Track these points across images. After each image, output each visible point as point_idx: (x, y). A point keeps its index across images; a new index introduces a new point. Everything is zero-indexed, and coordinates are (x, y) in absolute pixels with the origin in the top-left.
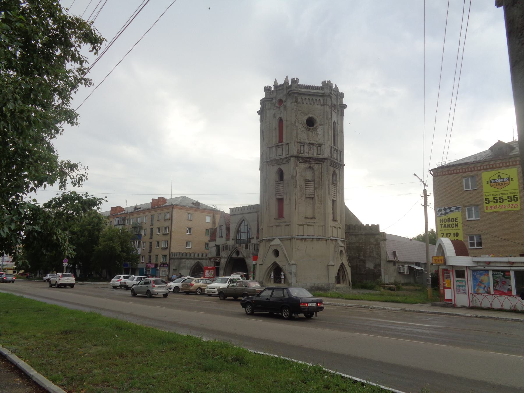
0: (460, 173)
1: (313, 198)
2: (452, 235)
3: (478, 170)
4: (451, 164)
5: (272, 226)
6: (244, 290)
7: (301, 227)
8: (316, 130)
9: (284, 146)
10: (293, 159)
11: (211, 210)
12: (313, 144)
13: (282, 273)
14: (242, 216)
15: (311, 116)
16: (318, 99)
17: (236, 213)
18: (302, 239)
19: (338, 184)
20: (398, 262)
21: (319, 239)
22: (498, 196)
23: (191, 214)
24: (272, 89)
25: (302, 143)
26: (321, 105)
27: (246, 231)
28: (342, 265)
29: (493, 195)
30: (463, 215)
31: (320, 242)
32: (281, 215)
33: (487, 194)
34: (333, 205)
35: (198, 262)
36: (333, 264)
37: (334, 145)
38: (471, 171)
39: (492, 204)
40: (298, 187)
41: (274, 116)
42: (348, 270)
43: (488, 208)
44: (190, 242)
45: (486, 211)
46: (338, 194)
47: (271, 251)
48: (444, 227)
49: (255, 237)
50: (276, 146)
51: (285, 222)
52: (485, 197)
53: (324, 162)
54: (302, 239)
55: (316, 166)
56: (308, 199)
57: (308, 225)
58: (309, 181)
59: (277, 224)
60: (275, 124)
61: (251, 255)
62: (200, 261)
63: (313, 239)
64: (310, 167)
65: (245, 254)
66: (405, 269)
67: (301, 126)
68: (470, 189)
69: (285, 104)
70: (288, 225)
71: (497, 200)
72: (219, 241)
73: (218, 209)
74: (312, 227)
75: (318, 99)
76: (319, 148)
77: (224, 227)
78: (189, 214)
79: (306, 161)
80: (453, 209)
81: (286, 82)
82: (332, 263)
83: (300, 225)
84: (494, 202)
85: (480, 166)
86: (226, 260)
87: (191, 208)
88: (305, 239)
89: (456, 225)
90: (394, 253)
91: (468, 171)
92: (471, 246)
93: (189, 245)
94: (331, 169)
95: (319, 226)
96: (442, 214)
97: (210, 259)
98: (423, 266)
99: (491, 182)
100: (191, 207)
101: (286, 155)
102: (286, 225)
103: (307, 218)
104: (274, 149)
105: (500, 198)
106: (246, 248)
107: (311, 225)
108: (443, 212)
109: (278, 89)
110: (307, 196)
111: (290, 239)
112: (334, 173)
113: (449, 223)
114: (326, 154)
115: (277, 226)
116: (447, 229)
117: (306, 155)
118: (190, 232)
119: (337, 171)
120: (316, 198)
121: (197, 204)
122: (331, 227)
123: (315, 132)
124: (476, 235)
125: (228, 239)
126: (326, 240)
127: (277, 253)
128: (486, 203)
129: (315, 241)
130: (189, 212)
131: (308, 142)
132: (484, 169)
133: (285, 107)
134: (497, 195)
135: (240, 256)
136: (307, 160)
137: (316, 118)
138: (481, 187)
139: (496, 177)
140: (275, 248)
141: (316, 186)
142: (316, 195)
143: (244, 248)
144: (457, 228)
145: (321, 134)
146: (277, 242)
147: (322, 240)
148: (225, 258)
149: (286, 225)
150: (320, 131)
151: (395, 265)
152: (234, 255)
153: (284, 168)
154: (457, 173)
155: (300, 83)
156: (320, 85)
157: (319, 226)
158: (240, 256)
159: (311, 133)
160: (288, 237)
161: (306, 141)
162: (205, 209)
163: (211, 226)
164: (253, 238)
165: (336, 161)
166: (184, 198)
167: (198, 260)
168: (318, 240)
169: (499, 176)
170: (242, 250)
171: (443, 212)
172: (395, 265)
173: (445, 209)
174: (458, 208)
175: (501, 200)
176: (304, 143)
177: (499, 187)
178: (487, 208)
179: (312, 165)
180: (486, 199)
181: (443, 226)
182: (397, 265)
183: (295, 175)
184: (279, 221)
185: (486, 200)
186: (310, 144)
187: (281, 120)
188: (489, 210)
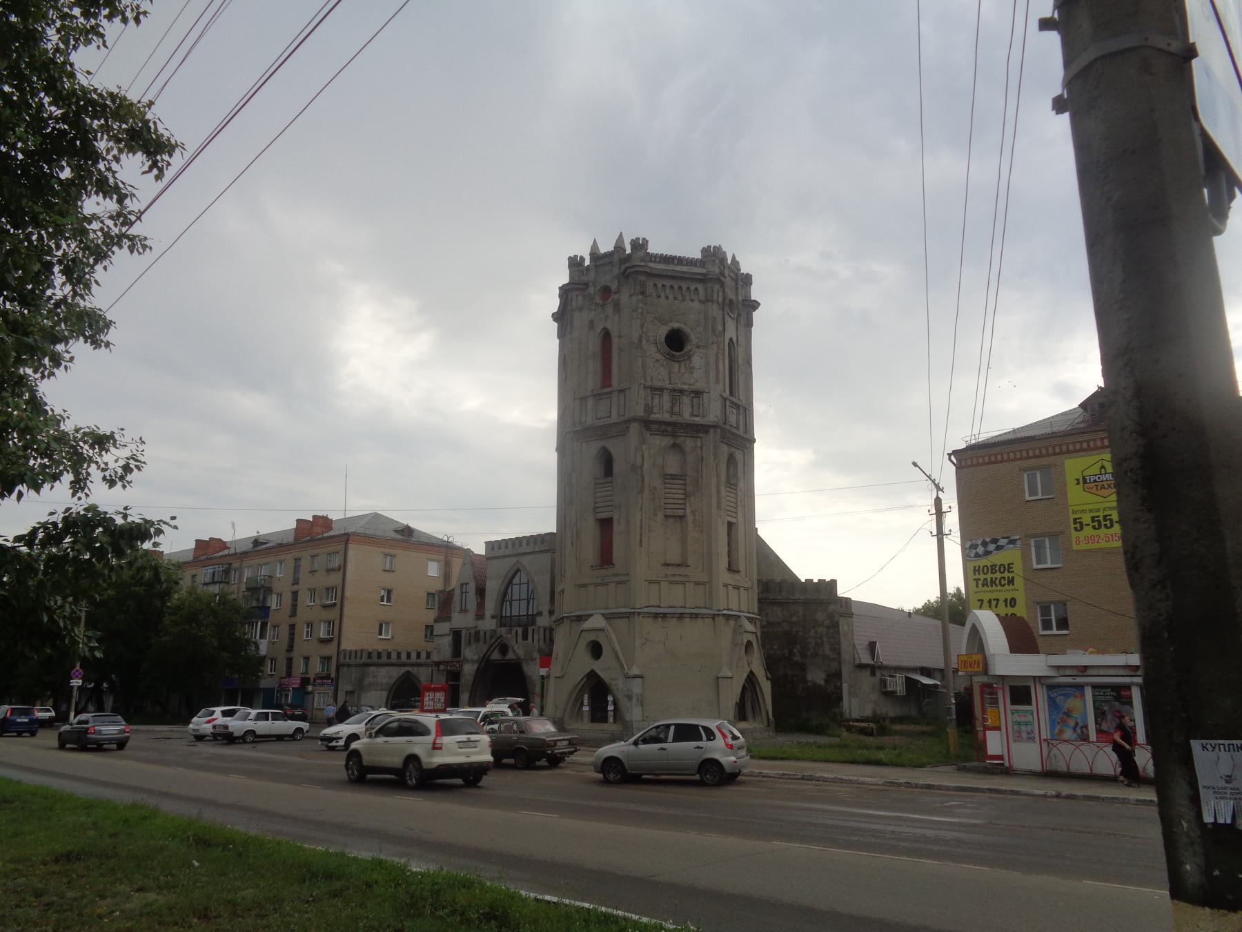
0: (1015, 459)
1: (682, 518)
2: (1001, 604)
3: (1055, 454)
4: (999, 439)
6: (517, 742)
7: (655, 586)
8: (689, 358)
9: (615, 396)
10: (634, 428)
11: (439, 546)
12: (682, 391)
13: (610, 698)
14: (514, 560)
15: (676, 325)
16: (692, 288)
17: (501, 553)
18: (656, 616)
19: (741, 485)
20: (882, 667)
22: (1101, 514)
23: (393, 556)
24: (587, 263)
25: (656, 389)
26: (700, 301)
27: (524, 596)
28: (751, 678)
29: (1091, 511)
30: (1026, 558)
31: (700, 621)
32: (606, 557)
33: (1076, 508)
34: (729, 535)
35: (408, 672)
36: (730, 674)
37: (731, 393)
38: (1041, 456)
39: (1088, 531)
40: (647, 491)
41: (591, 324)
42: (766, 687)
43: (1081, 541)
44: (387, 624)
45: (1075, 547)
46: (740, 509)
47: (583, 644)
49: (545, 609)
50: (594, 396)
51: (615, 575)
52: (1072, 516)
53: (707, 432)
54: (656, 616)
55: (689, 444)
56: (670, 520)
57: (671, 583)
58: (672, 477)
59: (599, 581)
60: (594, 344)
61: (536, 655)
62: (414, 670)
63: (681, 616)
64: (674, 446)
65: (521, 653)
66: (897, 685)
68: (1040, 496)
69: (616, 297)
71: (1099, 522)
72: (460, 620)
73: (459, 544)
74: (681, 586)
75: (692, 288)
76: (695, 400)
77: (472, 588)
78: (386, 555)
80: (1002, 542)
81: (619, 247)
83: (651, 582)
84: (1094, 527)
85: (1060, 446)
86: (475, 666)
87: (392, 543)
88: (664, 616)
89: (1011, 581)
90: (872, 646)
91: (1035, 457)
93: (387, 631)
94: (725, 449)
95: (697, 583)
96: (977, 555)
97: (438, 664)
98: (938, 675)
99: (1085, 481)
100: (393, 540)
101: (619, 416)
102: (620, 583)
103: (668, 565)
104: (590, 403)
105: (1105, 517)
106: (525, 637)
107: (676, 583)
108: (980, 550)
109: (601, 262)
110: (669, 512)
111: (628, 616)
112: (731, 459)
113: (994, 576)
114: (713, 414)
115: (597, 585)
116: (990, 588)
117: (667, 417)
118: (389, 600)
119: (739, 455)
120: (690, 518)
121: (407, 531)
122: (725, 585)
124: (1054, 603)
125: (480, 616)
126: (714, 617)
127: (596, 650)
128: (1076, 529)
129: (687, 620)
130: (387, 551)
131: (670, 387)
132: (1068, 452)
133: (617, 307)
134: (1098, 510)
135: (510, 656)
136: (669, 428)
137: (687, 330)
138: (1064, 493)
141: (689, 488)
142: (688, 510)
143: (520, 638)
144: (1011, 587)
145: (699, 368)
146: (597, 621)
147: (703, 616)
148: (473, 662)
149: (620, 583)
150: (697, 361)
151: (873, 674)
152: (496, 656)
153: (614, 447)
154: (1009, 460)
155: (653, 249)
156: (698, 256)
157: (697, 583)
158: (510, 656)
159: (676, 366)
160: (623, 610)
161: (666, 384)
162: (427, 544)
163: (439, 586)
164: (540, 614)
165: (735, 431)
166: (376, 517)
167: (407, 669)
168: (694, 616)
169: (1103, 467)
171: (980, 550)
172: (873, 674)
173: (985, 544)
174: (1013, 542)
175: (1108, 523)
176: (661, 390)
177: (1103, 492)
178: (1078, 539)
179: (679, 440)
180: (1075, 520)
182: (878, 674)
183: (639, 462)
184: (603, 572)
185: (1075, 523)
186: (674, 390)
187: (606, 336)
188: (1083, 546)
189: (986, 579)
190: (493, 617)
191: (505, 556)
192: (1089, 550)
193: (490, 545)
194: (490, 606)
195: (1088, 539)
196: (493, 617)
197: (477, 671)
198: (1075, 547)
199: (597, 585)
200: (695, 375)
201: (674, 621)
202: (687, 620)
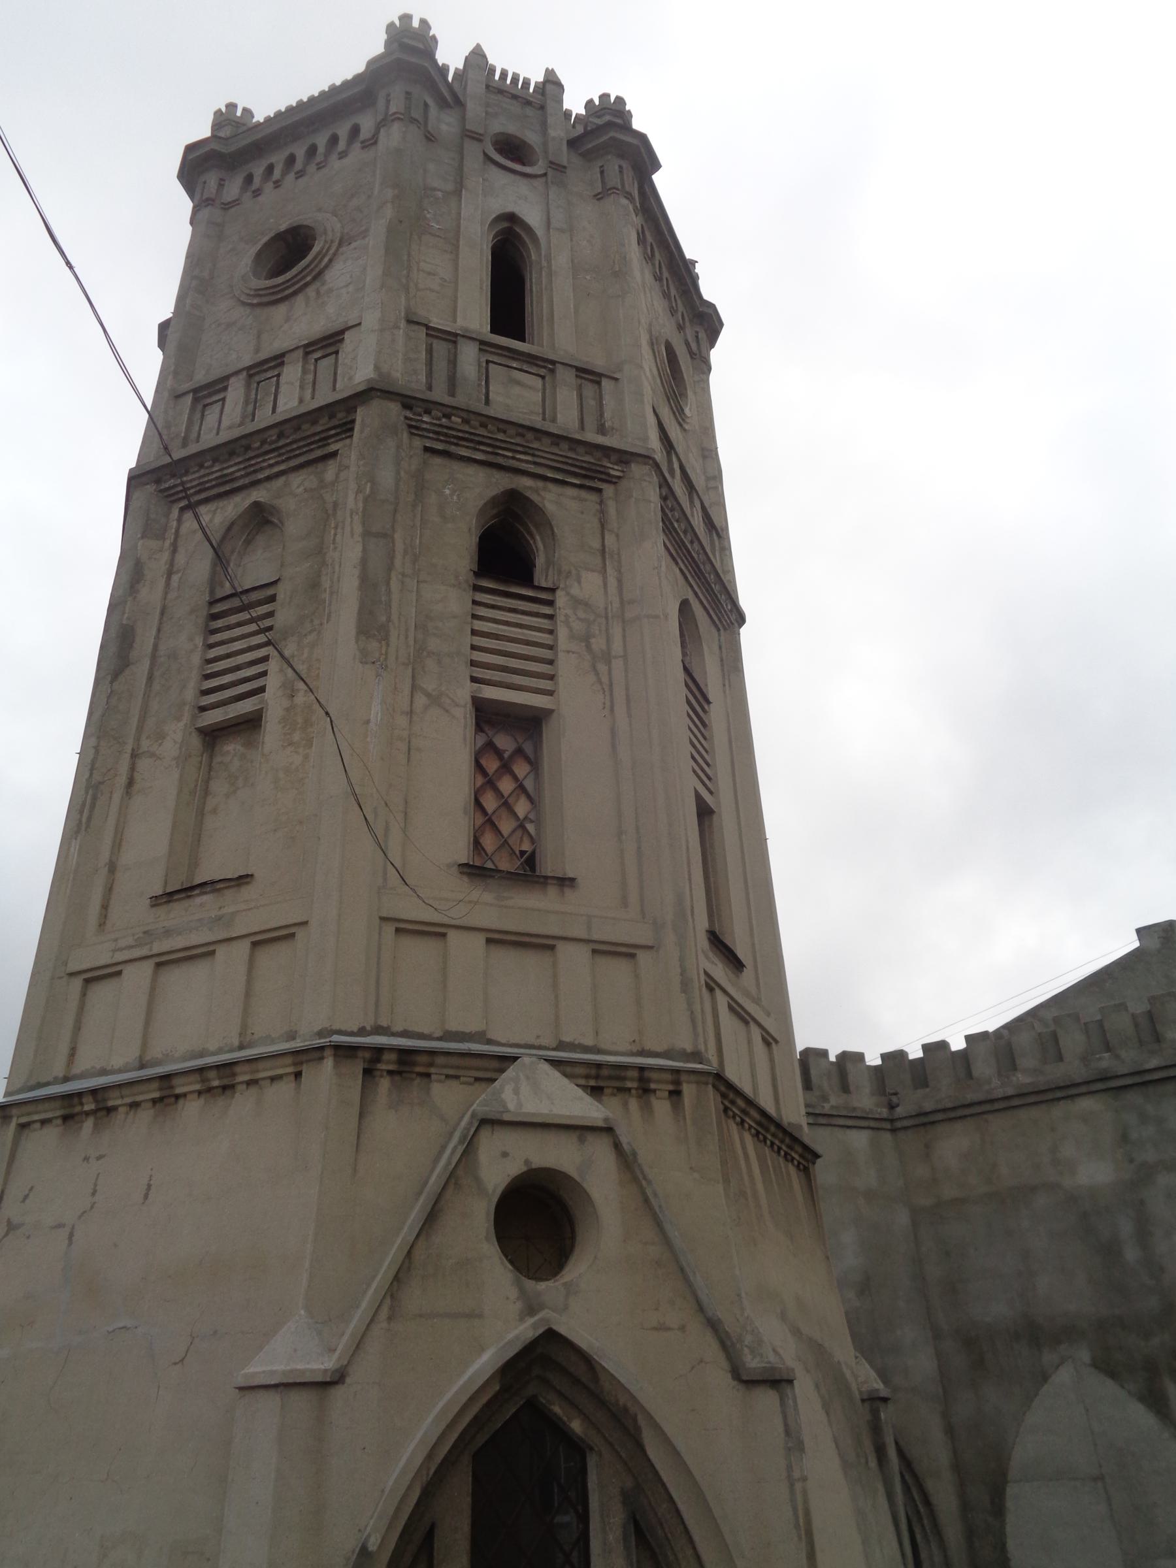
7: (102, 993)
12: (279, 360)
31: (243, 1103)
40: (141, 669)
46: (568, 667)
53: (347, 428)
56: (232, 748)
57: (163, 963)
63: (166, 1092)
74: (199, 971)
79: (224, 480)
82: (294, 1351)
95: (260, 942)
123: (311, 291)
136: (232, 468)
142: (273, 682)
200: (331, 309)
201: (146, 1114)
202: (192, 1108)
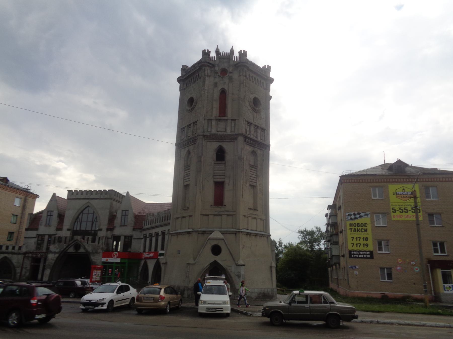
0: (368, 182)
2: (362, 239)
3: (384, 182)
4: (356, 174)
5: (207, 215)
6: (330, 309)
7: (246, 219)
9: (229, 122)
14: (87, 201)
15: (257, 96)
17: (78, 197)
21: (262, 235)
22: (403, 207)
24: (213, 54)
27: (90, 219)
29: (399, 205)
30: (372, 222)
32: (219, 201)
33: (393, 204)
35: (6, 257)
38: (378, 182)
39: (398, 213)
41: (216, 85)
43: (395, 217)
45: (393, 219)
48: (354, 231)
49: (104, 227)
50: (216, 120)
51: (228, 211)
52: (392, 207)
59: (216, 213)
61: (100, 251)
63: (256, 235)
65: (90, 249)
67: (247, 104)
68: (377, 198)
69: (230, 75)
70: (232, 215)
71: (402, 210)
72: (43, 230)
73: (32, 191)
74: (255, 220)
77: (55, 214)
79: (251, 144)
80: (362, 214)
83: (245, 216)
84: (400, 212)
85: (387, 179)
86: (57, 255)
89: (366, 230)
91: (376, 182)
92: (379, 250)
96: (351, 219)
99: (397, 194)
101: (231, 132)
102: (228, 215)
104: (214, 123)
105: (405, 208)
106: (94, 241)
108: (353, 217)
111: (236, 233)
113: (359, 228)
115: (215, 215)
116: (357, 233)
124: (384, 240)
128: (393, 212)
129: (258, 237)
132: (390, 182)
133: (231, 79)
134: (402, 206)
135: (82, 250)
138: (388, 197)
139: (401, 190)
140: (215, 243)
142: (258, 184)
143: (90, 242)
144: (366, 233)
146: (217, 234)
148: (55, 253)
149: (228, 215)
152: (71, 250)
153: (226, 146)
154: (365, 182)
158: (82, 250)
159: (255, 114)
160: (232, 230)
163: (18, 212)
164: (101, 230)
167: (5, 255)
169: (403, 189)
170: (85, 244)
171: (353, 217)
173: (355, 214)
174: (367, 215)
175: (394, 211)
177: (404, 199)
178: (394, 216)
179: (256, 149)
180: (393, 209)
181: (353, 230)
184: (218, 209)
185: (393, 209)
187: (223, 93)
188: (396, 219)
189: (355, 229)
190: (68, 230)
191: (80, 199)
192: (399, 221)
193: (70, 192)
194: (67, 224)
195: (398, 216)
196: (68, 230)
197: (57, 258)
198: (393, 219)
199: (215, 215)
201: (254, 237)
